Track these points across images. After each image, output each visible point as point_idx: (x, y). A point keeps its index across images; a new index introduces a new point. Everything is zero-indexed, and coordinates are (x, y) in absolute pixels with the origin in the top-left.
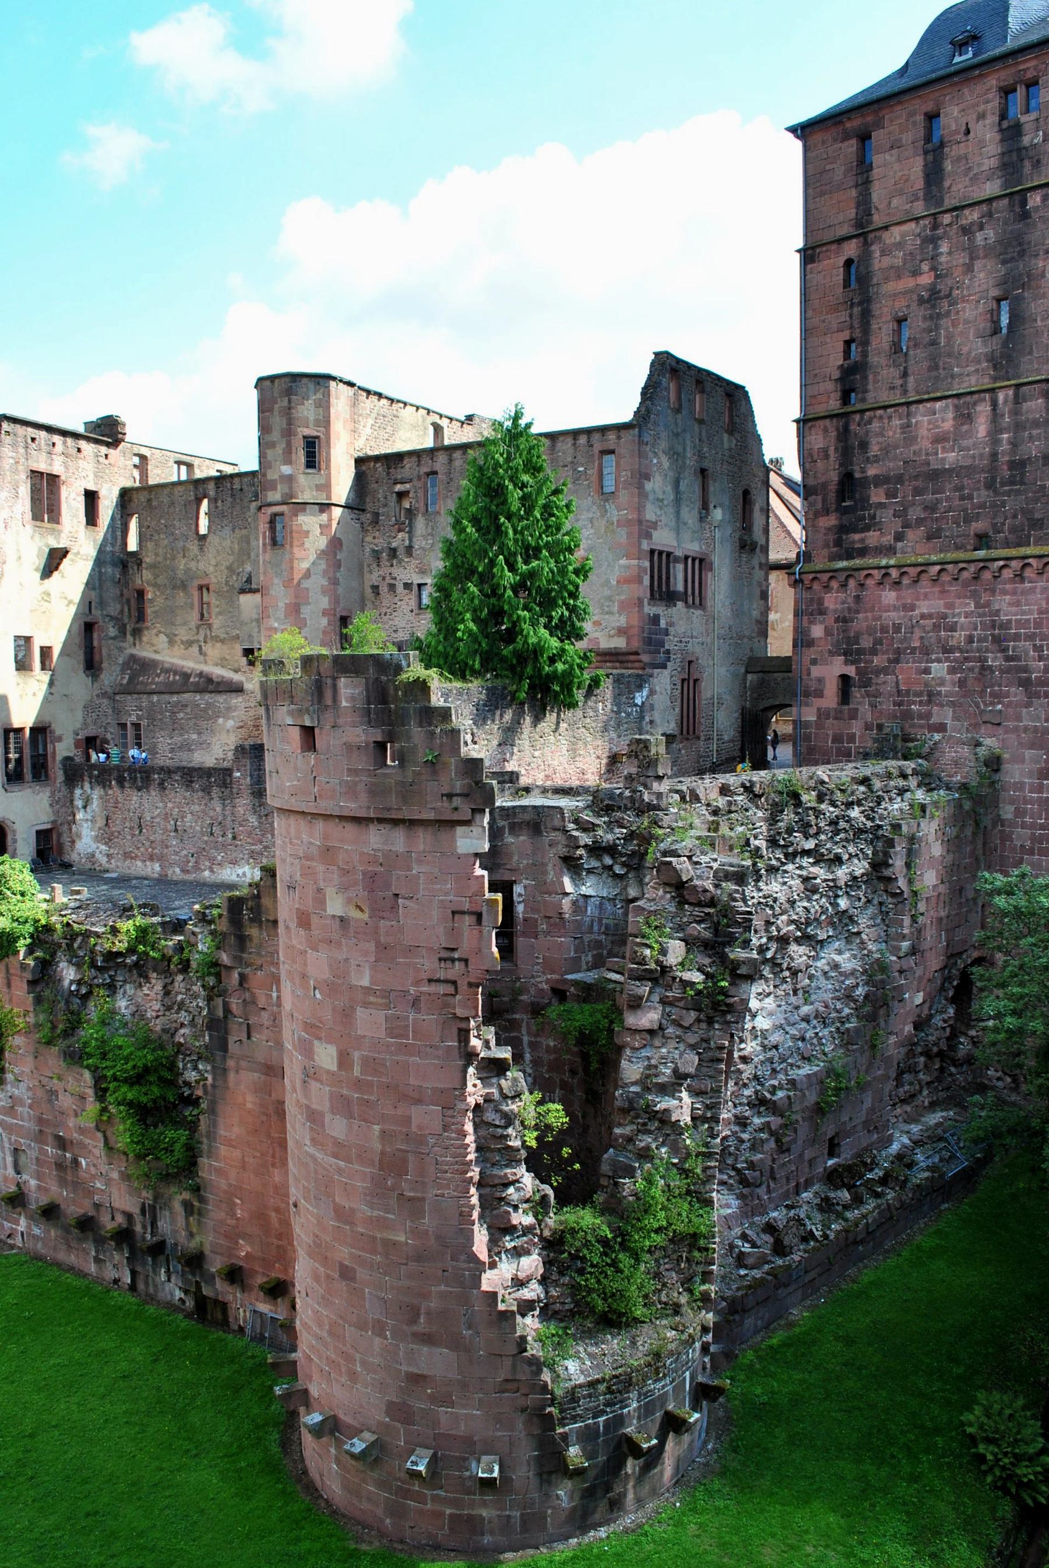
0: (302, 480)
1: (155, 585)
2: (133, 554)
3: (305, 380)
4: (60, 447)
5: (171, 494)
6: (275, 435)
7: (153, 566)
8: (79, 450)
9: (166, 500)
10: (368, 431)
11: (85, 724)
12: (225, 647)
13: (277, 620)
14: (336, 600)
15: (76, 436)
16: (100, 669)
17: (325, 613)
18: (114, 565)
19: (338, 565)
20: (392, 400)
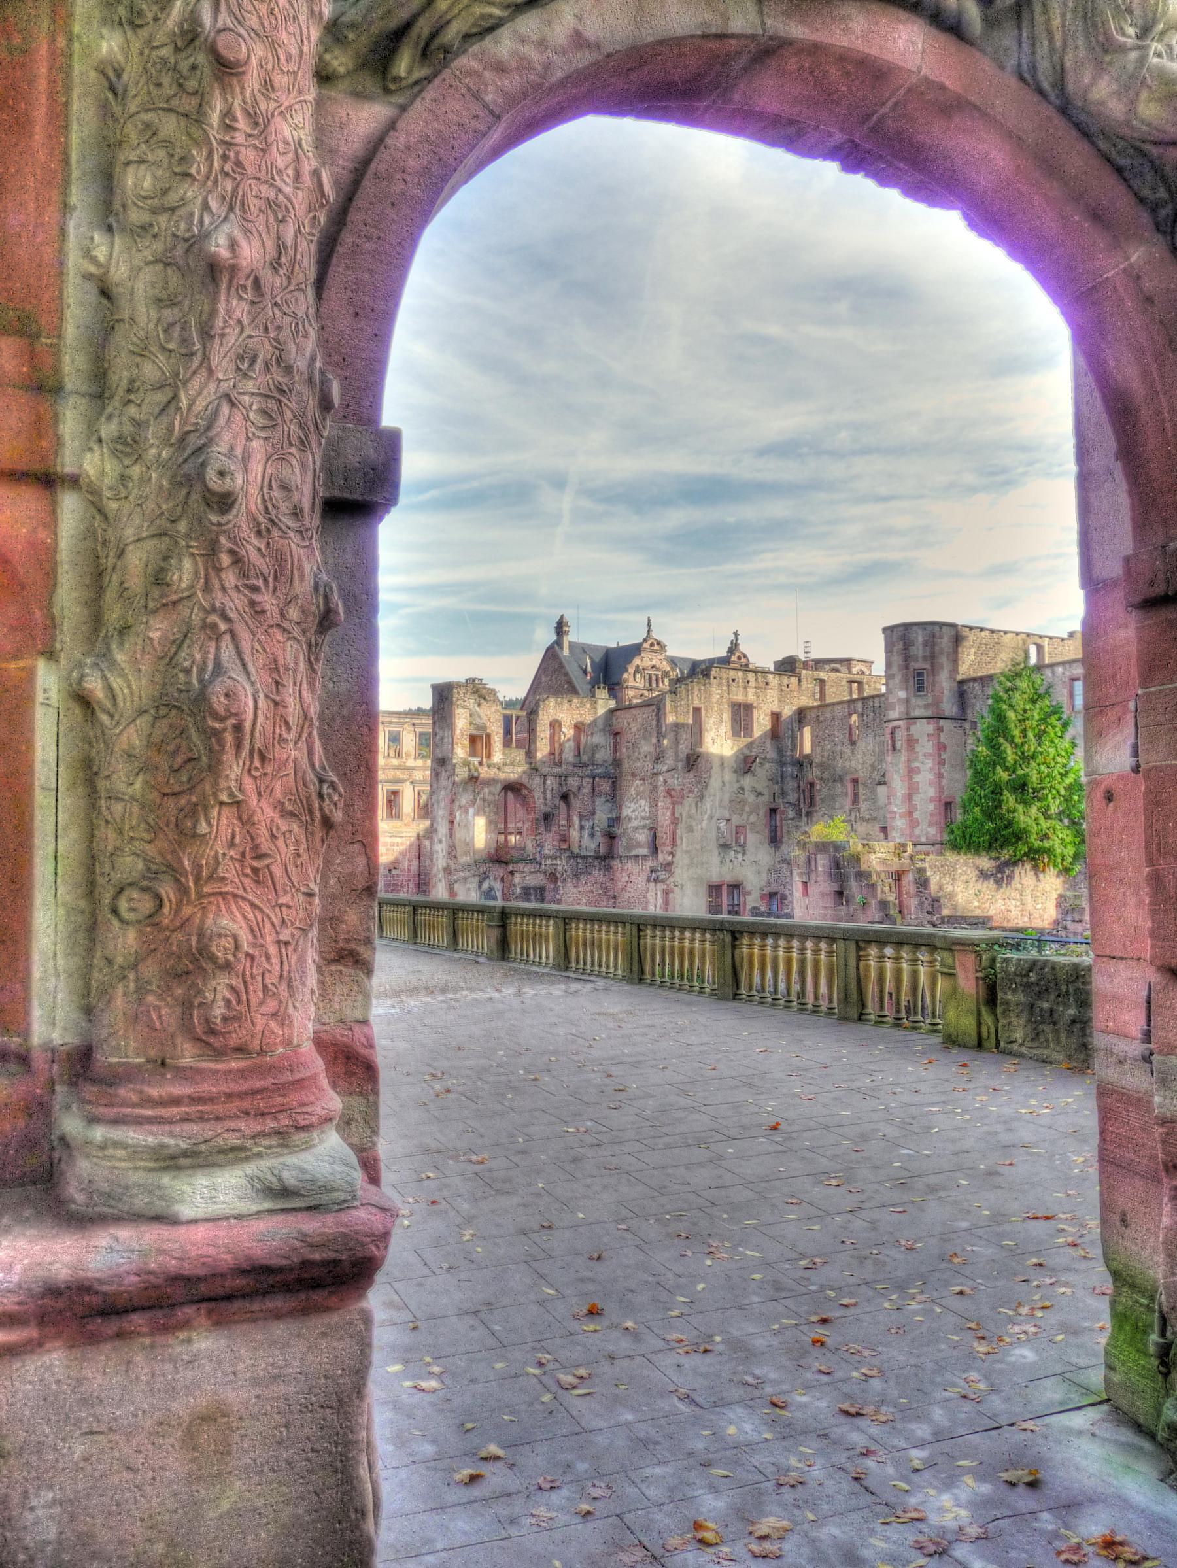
0: (913, 701)
1: (821, 779)
2: (808, 756)
3: (915, 628)
4: (752, 683)
5: (832, 711)
6: (895, 670)
7: (821, 765)
8: (767, 684)
9: (829, 716)
10: (972, 657)
11: (769, 883)
12: (869, 825)
13: (896, 805)
14: (941, 790)
15: (764, 672)
16: (781, 842)
17: (931, 800)
18: (793, 764)
19: (942, 763)
20: (993, 632)
